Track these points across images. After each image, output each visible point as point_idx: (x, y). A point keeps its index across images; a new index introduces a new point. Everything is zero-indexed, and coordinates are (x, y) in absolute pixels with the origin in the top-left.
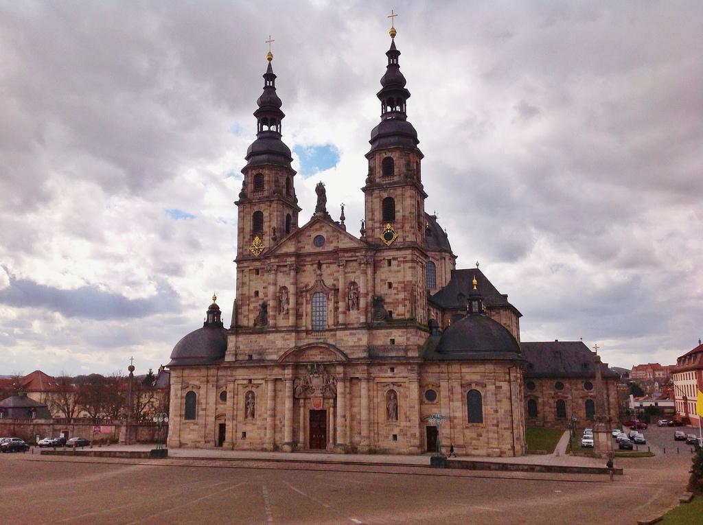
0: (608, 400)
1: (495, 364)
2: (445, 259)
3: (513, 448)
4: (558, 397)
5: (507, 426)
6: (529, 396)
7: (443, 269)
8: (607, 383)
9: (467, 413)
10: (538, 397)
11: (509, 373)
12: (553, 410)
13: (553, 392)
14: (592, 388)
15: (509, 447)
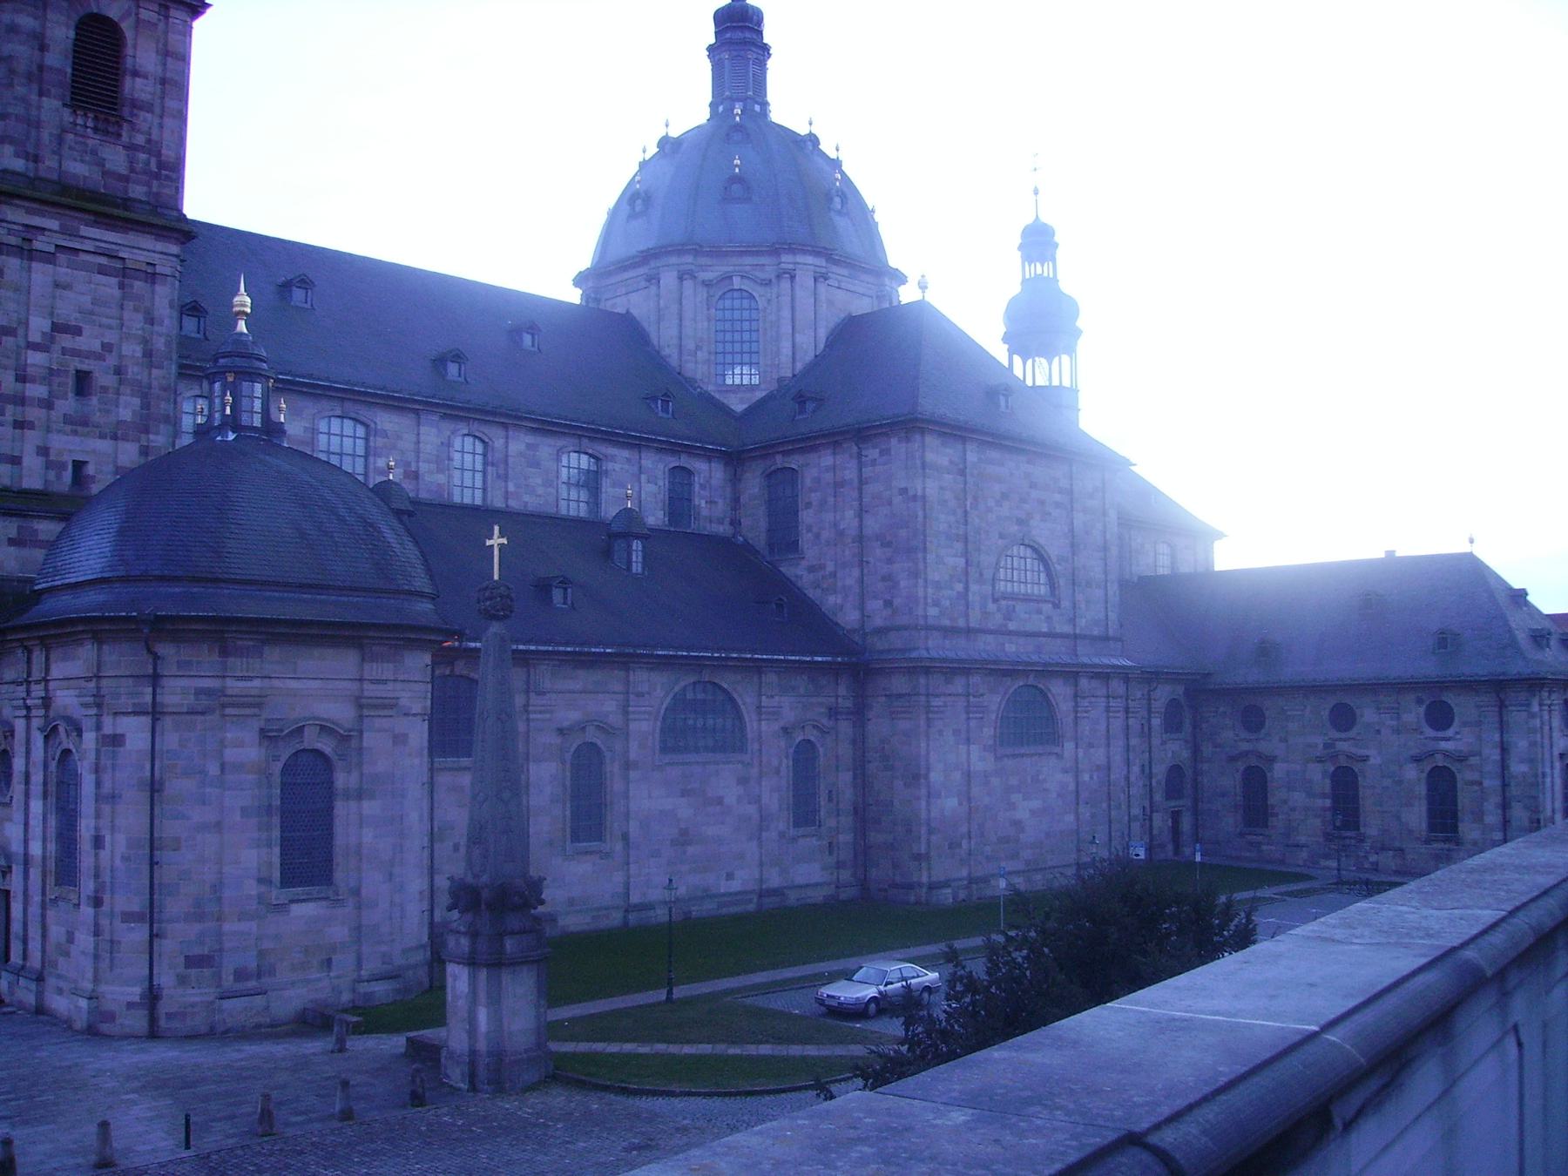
0: (1504, 765)
1: (99, 638)
2: (793, 278)
3: (152, 996)
4: (1334, 757)
5: (136, 908)
6: (1246, 754)
7: (786, 313)
8: (1502, 706)
9: (52, 847)
10: (1272, 760)
11: (155, 679)
12: (1319, 802)
13: (1319, 741)
14: (1449, 725)
15: (135, 992)
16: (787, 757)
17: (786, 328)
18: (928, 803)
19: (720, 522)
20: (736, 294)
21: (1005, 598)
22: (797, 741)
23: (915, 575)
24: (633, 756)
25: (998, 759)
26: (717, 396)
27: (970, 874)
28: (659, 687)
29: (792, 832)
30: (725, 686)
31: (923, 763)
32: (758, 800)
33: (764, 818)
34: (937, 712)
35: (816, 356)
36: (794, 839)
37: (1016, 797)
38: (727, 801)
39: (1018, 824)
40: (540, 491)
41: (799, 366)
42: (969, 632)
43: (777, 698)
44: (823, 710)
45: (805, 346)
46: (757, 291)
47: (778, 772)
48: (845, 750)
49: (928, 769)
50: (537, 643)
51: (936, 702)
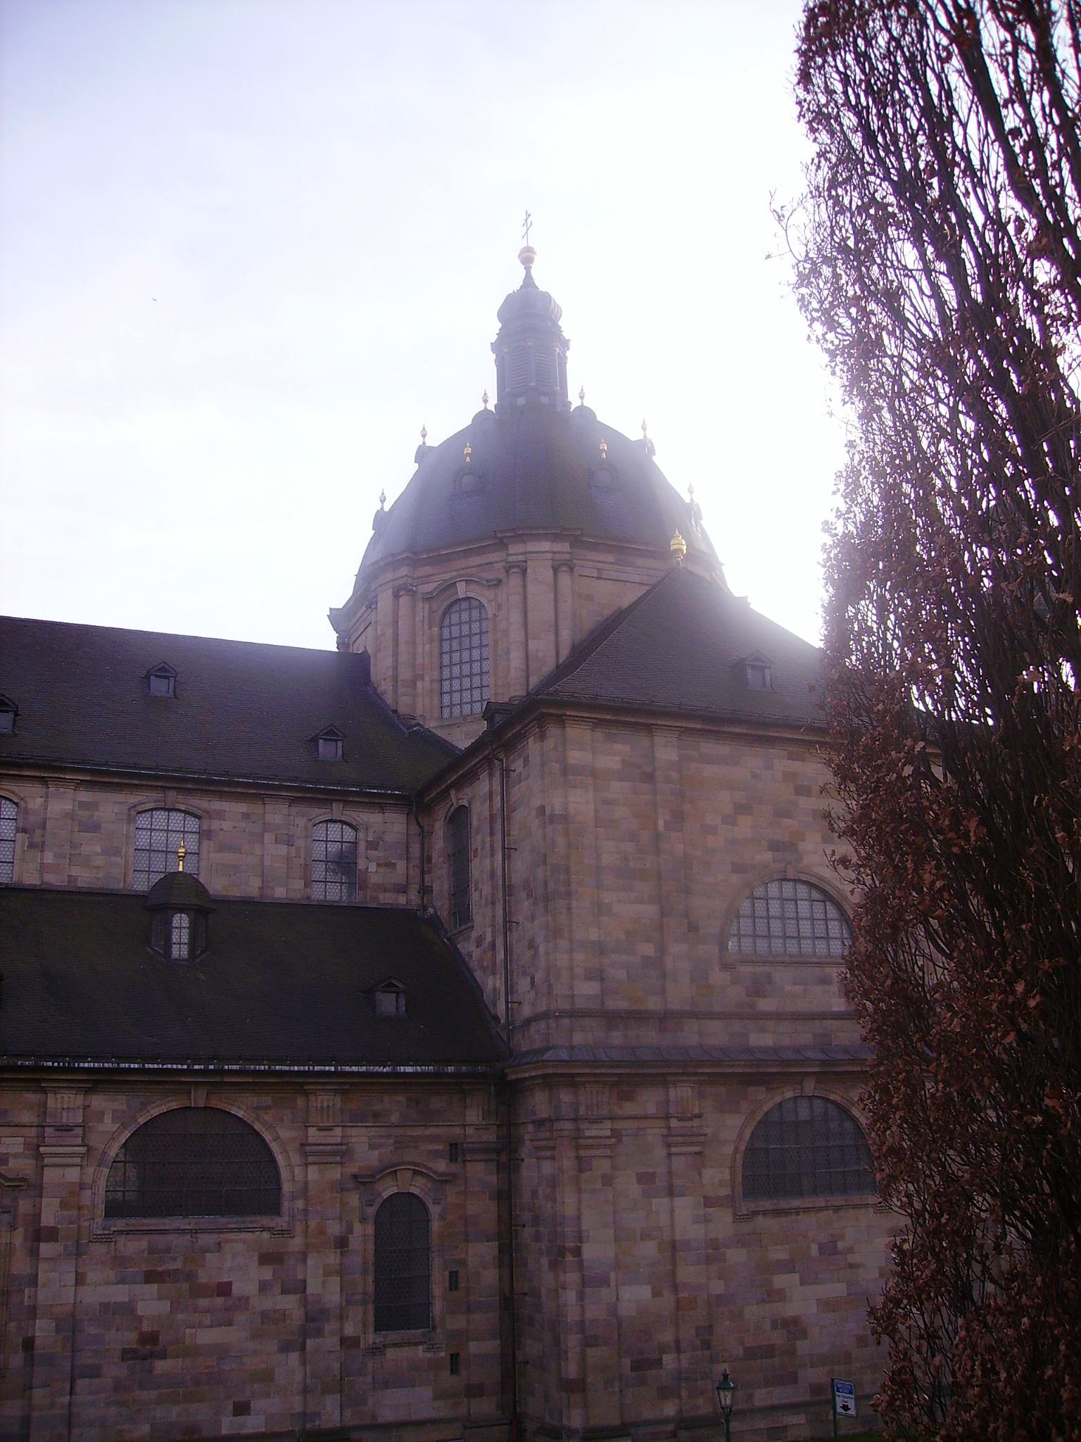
7: (516, 617)
16: (363, 1220)
17: (516, 635)
18: (581, 1296)
19: (403, 889)
20: (464, 605)
21: (742, 962)
22: (385, 1195)
23: (555, 933)
24: (47, 1220)
25: (738, 1218)
26: (439, 733)
27: (680, 1411)
28: (108, 1119)
29: (371, 1338)
30: (240, 1114)
31: (569, 1230)
32: (301, 1287)
33: (314, 1319)
34: (591, 1147)
35: (557, 667)
36: (376, 1350)
37: (780, 1281)
38: (236, 1290)
39: (794, 1327)
40: (99, 861)
41: (534, 680)
42: (666, 1019)
43: (338, 1131)
44: (441, 1147)
45: (540, 654)
46: (484, 596)
47: (342, 1243)
48: (483, 1209)
49: (580, 1238)
50: (96, 1059)
51: (591, 1131)
